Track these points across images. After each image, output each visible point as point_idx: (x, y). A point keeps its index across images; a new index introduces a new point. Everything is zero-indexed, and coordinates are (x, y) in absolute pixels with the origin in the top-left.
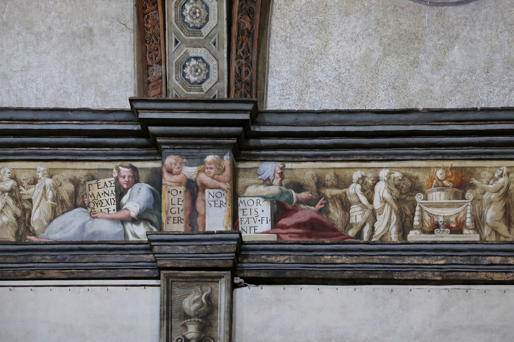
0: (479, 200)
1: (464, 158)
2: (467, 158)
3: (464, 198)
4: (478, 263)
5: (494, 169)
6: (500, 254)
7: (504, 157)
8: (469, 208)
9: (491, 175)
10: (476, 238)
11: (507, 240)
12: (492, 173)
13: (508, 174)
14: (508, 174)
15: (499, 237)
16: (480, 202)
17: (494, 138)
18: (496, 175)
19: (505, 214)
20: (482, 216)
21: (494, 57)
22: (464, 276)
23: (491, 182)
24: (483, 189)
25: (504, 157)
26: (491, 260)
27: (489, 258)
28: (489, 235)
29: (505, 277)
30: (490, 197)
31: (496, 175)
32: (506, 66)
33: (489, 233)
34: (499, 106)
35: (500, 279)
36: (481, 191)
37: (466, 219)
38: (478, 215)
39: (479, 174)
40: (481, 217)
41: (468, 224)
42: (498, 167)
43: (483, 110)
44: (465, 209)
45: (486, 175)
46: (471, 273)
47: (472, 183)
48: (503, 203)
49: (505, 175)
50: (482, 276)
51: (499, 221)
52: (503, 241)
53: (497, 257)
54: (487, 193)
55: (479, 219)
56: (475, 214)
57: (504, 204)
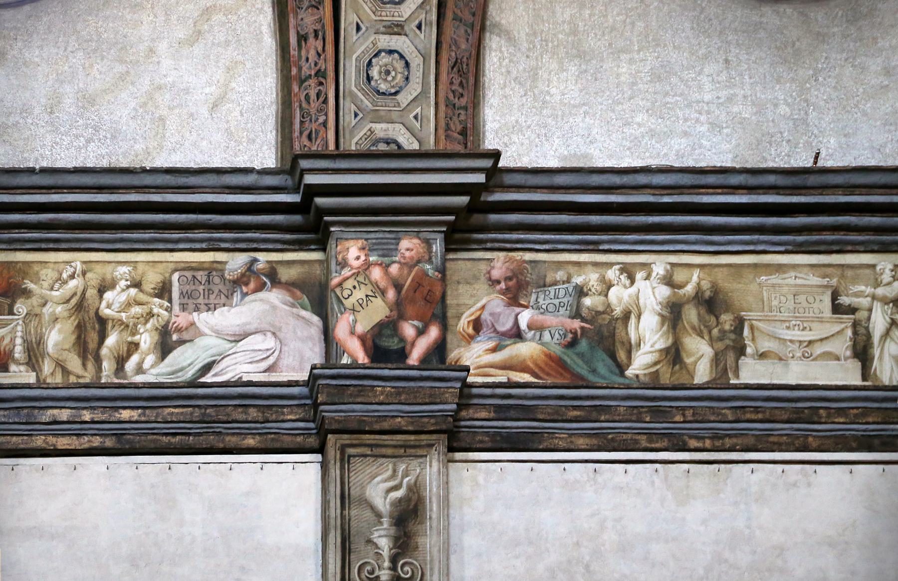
0: (36, 315)
1: (12, 247)
2: (18, 247)
3: (11, 313)
4: (33, 420)
5: (62, 266)
6: (68, 404)
7: (77, 246)
8: (19, 328)
9: (55, 275)
10: (31, 378)
11: (81, 381)
12: (58, 271)
13: (84, 273)
14: (84, 273)
15: (68, 377)
16: (37, 319)
17: (61, 216)
18: (65, 276)
19: (79, 337)
20: (40, 342)
21: (61, 90)
22: (8, 443)
23: (57, 286)
24: (43, 298)
25: (77, 246)
26: (54, 415)
27: (50, 412)
28: (52, 374)
29: (77, 443)
30: (54, 311)
31: (65, 276)
32: (80, 104)
33: (51, 371)
34: (70, 165)
35: (68, 447)
36: (40, 301)
37: (14, 346)
38: (34, 340)
39: (37, 273)
40: (39, 344)
41: (17, 355)
42: (68, 263)
43: (44, 171)
44: (14, 330)
45: (48, 274)
46: (21, 438)
47: (26, 289)
48: (75, 320)
49: (78, 276)
50: (39, 442)
51: (69, 350)
52: (73, 383)
53: (63, 410)
54: (49, 305)
55: (35, 346)
56: (29, 339)
57: (77, 322)
